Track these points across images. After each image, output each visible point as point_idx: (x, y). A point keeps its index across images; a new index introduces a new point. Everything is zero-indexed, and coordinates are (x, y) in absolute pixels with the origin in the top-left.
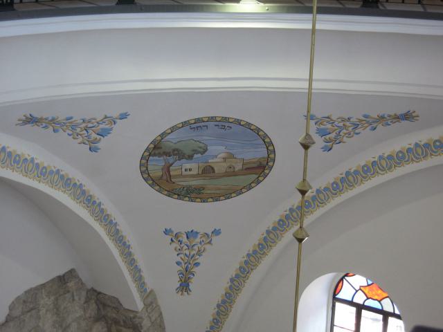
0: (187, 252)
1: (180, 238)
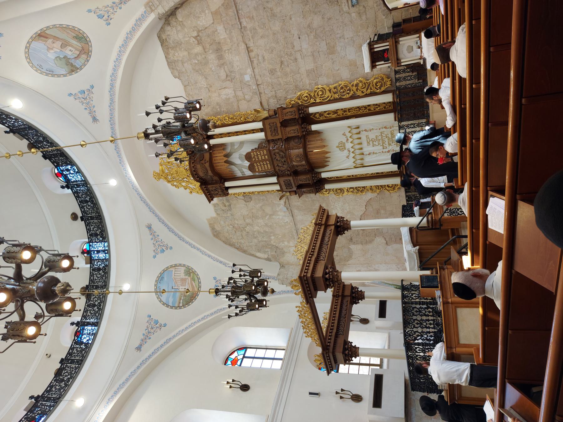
0: (111, 10)
1: (107, 18)
